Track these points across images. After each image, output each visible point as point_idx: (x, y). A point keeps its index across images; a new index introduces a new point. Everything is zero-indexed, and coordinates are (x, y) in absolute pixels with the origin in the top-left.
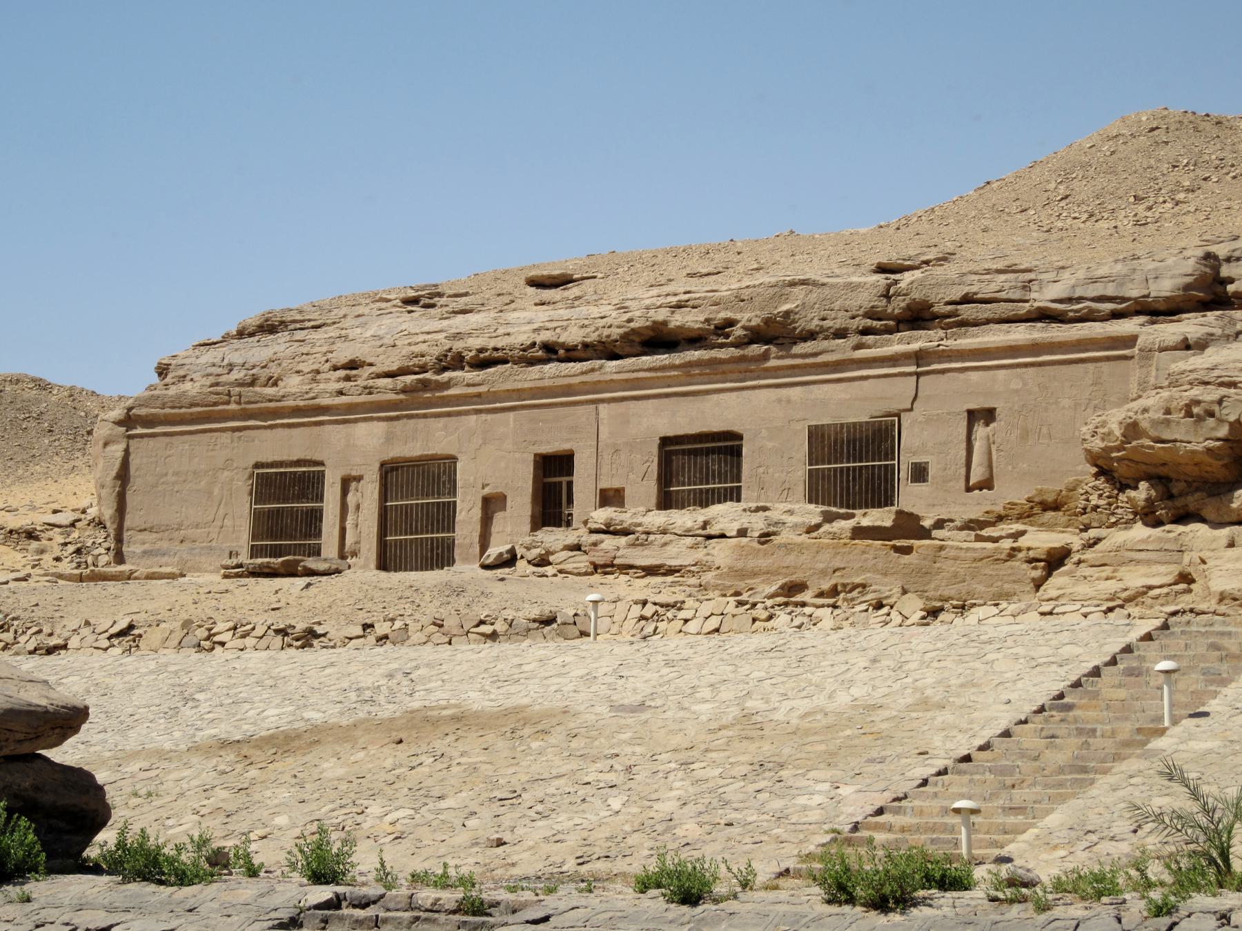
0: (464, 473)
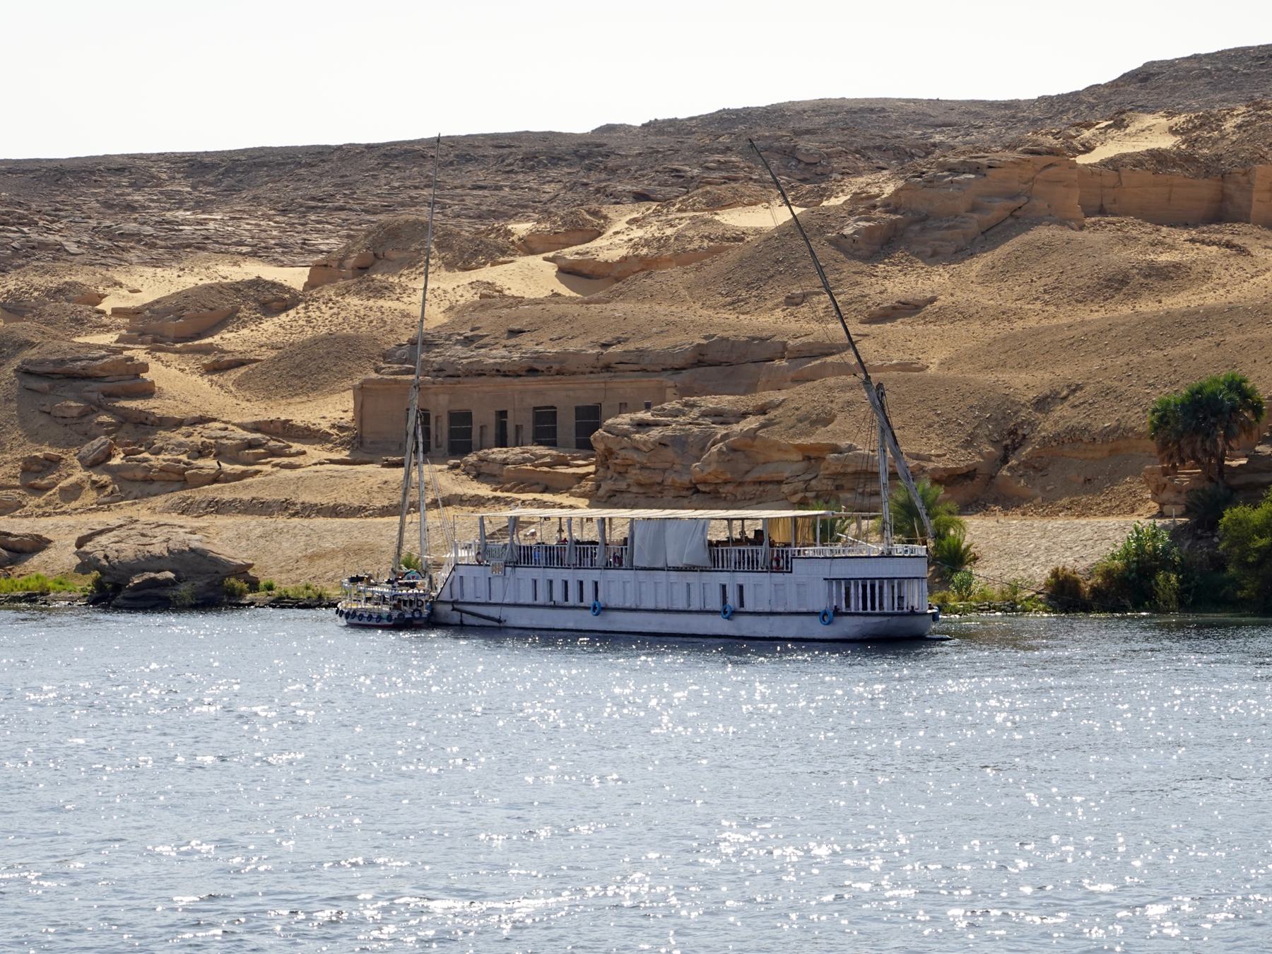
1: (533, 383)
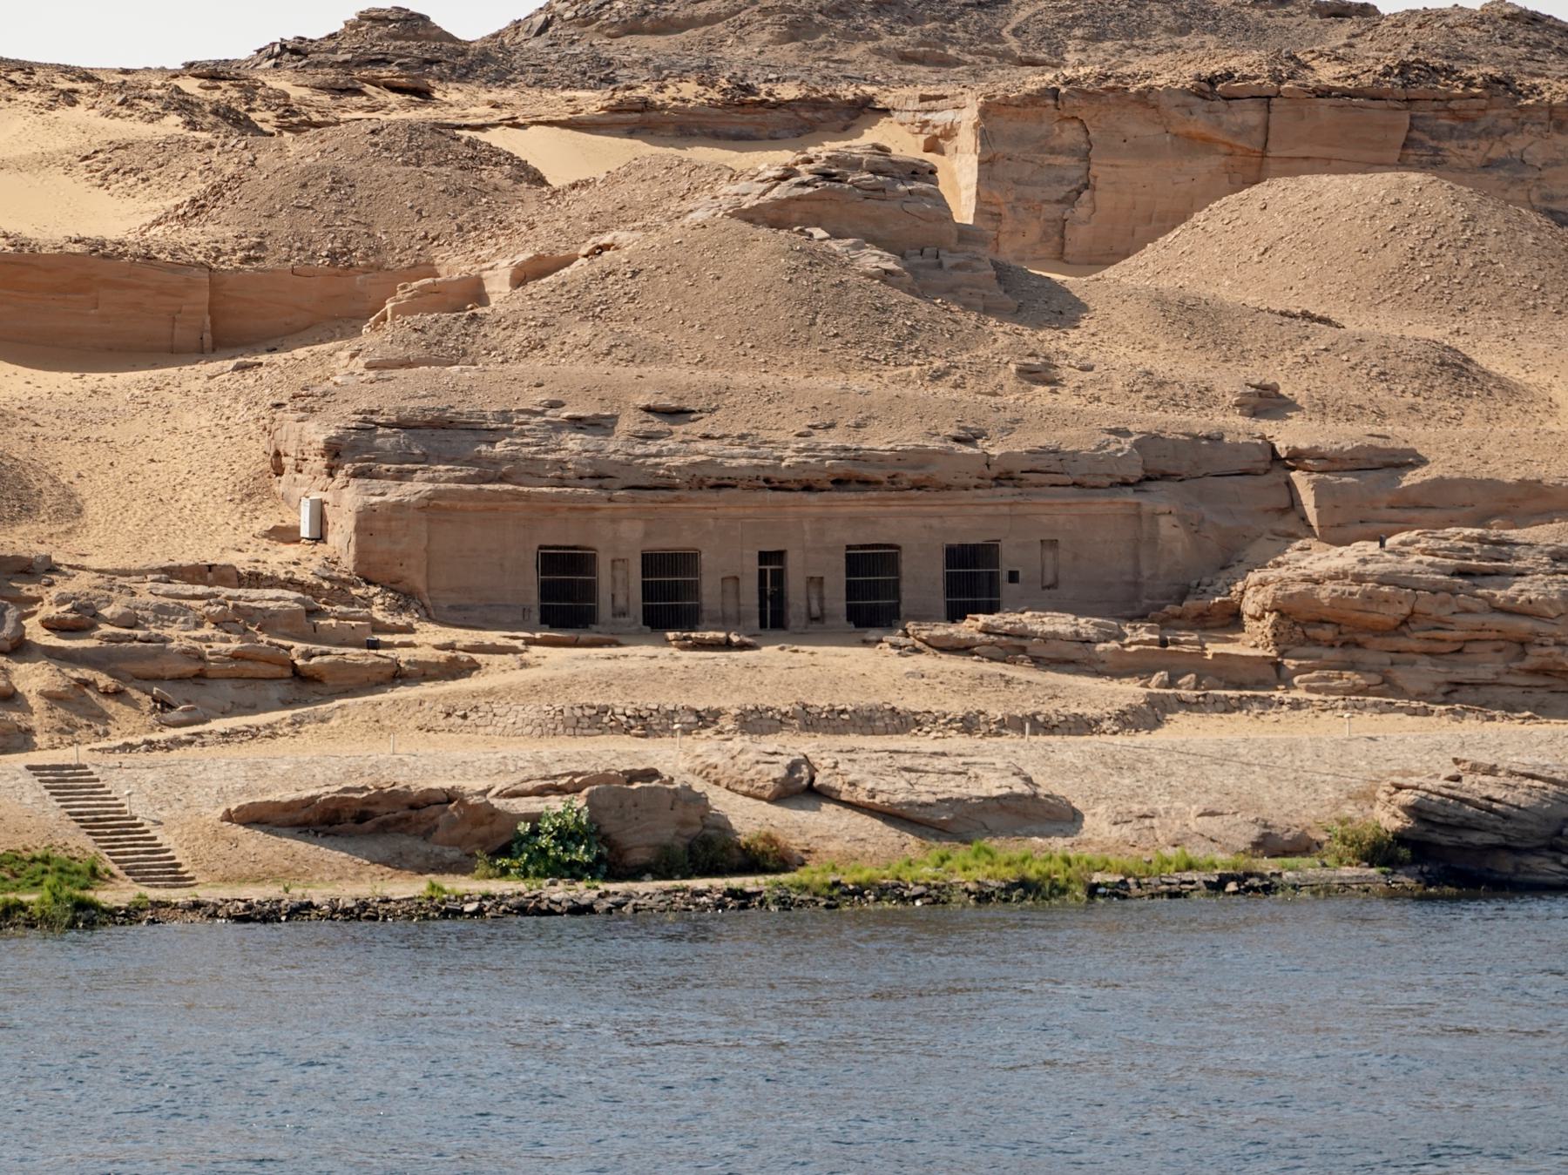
1: (850, 503)
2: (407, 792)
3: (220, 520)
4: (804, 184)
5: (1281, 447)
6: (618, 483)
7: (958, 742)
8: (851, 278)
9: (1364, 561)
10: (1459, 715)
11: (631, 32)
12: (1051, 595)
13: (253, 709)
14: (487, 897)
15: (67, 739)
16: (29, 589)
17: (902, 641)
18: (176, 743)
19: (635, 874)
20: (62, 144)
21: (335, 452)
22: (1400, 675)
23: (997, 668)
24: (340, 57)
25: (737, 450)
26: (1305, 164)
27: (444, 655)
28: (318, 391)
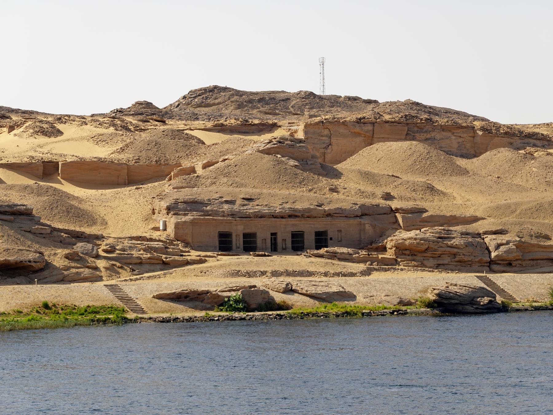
0: (258, 235)
1: (292, 221)
2: (197, 291)
3: (140, 225)
4: (274, 144)
5: (393, 207)
6: (237, 216)
7: (324, 279)
8: (288, 167)
9: (416, 235)
10: (441, 272)
11: (199, 107)
12: (340, 243)
13: (154, 271)
14: (220, 316)
15: (111, 278)
16: (99, 242)
17: (307, 254)
18: (137, 279)
19: (253, 310)
20: (86, 134)
21: (169, 209)
22: (425, 262)
23: (330, 261)
24: (131, 113)
25: (265, 208)
26: (383, 139)
27: (198, 258)
28: (163, 194)
